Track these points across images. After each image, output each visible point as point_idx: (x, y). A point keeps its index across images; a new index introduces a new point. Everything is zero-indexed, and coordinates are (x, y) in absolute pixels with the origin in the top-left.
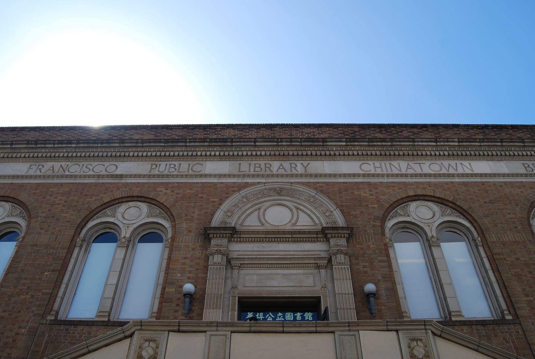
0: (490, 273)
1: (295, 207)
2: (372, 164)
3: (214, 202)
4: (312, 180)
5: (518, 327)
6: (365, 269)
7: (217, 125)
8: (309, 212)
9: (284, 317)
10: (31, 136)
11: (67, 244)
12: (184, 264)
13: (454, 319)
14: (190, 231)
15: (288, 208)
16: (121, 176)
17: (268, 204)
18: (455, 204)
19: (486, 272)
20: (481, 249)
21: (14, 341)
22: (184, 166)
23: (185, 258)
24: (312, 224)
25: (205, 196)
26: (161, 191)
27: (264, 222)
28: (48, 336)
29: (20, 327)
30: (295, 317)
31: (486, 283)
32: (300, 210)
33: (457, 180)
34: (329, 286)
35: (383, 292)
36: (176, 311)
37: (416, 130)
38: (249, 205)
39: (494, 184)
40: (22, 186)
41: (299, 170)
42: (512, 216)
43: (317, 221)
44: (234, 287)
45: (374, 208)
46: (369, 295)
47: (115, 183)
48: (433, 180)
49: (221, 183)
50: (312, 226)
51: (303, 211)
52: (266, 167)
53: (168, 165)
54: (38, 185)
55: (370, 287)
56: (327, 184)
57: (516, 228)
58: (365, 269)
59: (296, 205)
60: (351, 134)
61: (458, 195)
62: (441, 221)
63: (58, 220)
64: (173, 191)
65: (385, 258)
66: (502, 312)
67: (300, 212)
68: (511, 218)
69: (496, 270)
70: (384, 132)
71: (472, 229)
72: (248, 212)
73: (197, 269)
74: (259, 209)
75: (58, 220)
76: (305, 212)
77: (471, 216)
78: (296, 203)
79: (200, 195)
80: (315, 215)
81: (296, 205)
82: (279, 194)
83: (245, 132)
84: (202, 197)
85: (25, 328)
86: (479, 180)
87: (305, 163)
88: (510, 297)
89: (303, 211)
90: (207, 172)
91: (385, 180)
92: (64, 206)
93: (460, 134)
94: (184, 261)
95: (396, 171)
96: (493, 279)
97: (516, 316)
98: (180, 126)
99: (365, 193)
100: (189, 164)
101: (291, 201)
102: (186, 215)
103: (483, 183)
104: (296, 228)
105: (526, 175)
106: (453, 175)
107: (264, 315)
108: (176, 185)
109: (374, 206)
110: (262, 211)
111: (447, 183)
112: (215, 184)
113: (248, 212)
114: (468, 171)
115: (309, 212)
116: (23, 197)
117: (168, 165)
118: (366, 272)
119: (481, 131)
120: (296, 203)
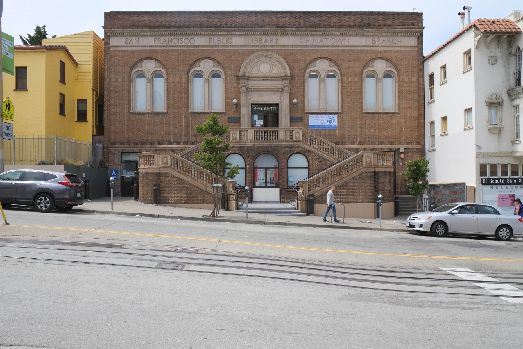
2: (305, 39)
3: (239, 60)
6: (295, 92)
7: (236, 12)
9: (266, 109)
10: (147, 19)
11: (186, 82)
12: (231, 90)
15: (268, 63)
16: (198, 46)
17: (261, 62)
18: (335, 62)
21: (181, 120)
22: (224, 39)
23: (231, 87)
25: (235, 57)
26: (217, 54)
29: (181, 115)
30: (270, 109)
33: (340, 49)
35: (300, 101)
36: (231, 108)
37: (329, 15)
38: (254, 63)
39: (355, 51)
40: (155, 51)
41: (274, 42)
42: (357, 68)
43: (280, 72)
45: (302, 64)
47: (196, 50)
48: (330, 49)
49: (241, 50)
54: (163, 50)
55: (295, 101)
57: (356, 74)
58: (295, 92)
64: (221, 55)
67: (273, 66)
68: (356, 70)
73: (236, 92)
76: (275, 66)
78: (272, 62)
79: (233, 57)
81: (272, 62)
83: (250, 16)
84: (234, 58)
87: (277, 38)
90: (234, 44)
91: (310, 48)
92: (178, 63)
94: (231, 88)
95: (315, 44)
98: (218, 12)
99: (300, 56)
102: (229, 67)
103: (351, 51)
104: (271, 74)
105: (371, 46)
106: (339, 46)
107: (260, 108)
108: (222, 51)
110: (259, 65)
111: (335, 50)
114: (346, 44)
116: (158, 58)
118: (295, 93)
120: (272, 62)
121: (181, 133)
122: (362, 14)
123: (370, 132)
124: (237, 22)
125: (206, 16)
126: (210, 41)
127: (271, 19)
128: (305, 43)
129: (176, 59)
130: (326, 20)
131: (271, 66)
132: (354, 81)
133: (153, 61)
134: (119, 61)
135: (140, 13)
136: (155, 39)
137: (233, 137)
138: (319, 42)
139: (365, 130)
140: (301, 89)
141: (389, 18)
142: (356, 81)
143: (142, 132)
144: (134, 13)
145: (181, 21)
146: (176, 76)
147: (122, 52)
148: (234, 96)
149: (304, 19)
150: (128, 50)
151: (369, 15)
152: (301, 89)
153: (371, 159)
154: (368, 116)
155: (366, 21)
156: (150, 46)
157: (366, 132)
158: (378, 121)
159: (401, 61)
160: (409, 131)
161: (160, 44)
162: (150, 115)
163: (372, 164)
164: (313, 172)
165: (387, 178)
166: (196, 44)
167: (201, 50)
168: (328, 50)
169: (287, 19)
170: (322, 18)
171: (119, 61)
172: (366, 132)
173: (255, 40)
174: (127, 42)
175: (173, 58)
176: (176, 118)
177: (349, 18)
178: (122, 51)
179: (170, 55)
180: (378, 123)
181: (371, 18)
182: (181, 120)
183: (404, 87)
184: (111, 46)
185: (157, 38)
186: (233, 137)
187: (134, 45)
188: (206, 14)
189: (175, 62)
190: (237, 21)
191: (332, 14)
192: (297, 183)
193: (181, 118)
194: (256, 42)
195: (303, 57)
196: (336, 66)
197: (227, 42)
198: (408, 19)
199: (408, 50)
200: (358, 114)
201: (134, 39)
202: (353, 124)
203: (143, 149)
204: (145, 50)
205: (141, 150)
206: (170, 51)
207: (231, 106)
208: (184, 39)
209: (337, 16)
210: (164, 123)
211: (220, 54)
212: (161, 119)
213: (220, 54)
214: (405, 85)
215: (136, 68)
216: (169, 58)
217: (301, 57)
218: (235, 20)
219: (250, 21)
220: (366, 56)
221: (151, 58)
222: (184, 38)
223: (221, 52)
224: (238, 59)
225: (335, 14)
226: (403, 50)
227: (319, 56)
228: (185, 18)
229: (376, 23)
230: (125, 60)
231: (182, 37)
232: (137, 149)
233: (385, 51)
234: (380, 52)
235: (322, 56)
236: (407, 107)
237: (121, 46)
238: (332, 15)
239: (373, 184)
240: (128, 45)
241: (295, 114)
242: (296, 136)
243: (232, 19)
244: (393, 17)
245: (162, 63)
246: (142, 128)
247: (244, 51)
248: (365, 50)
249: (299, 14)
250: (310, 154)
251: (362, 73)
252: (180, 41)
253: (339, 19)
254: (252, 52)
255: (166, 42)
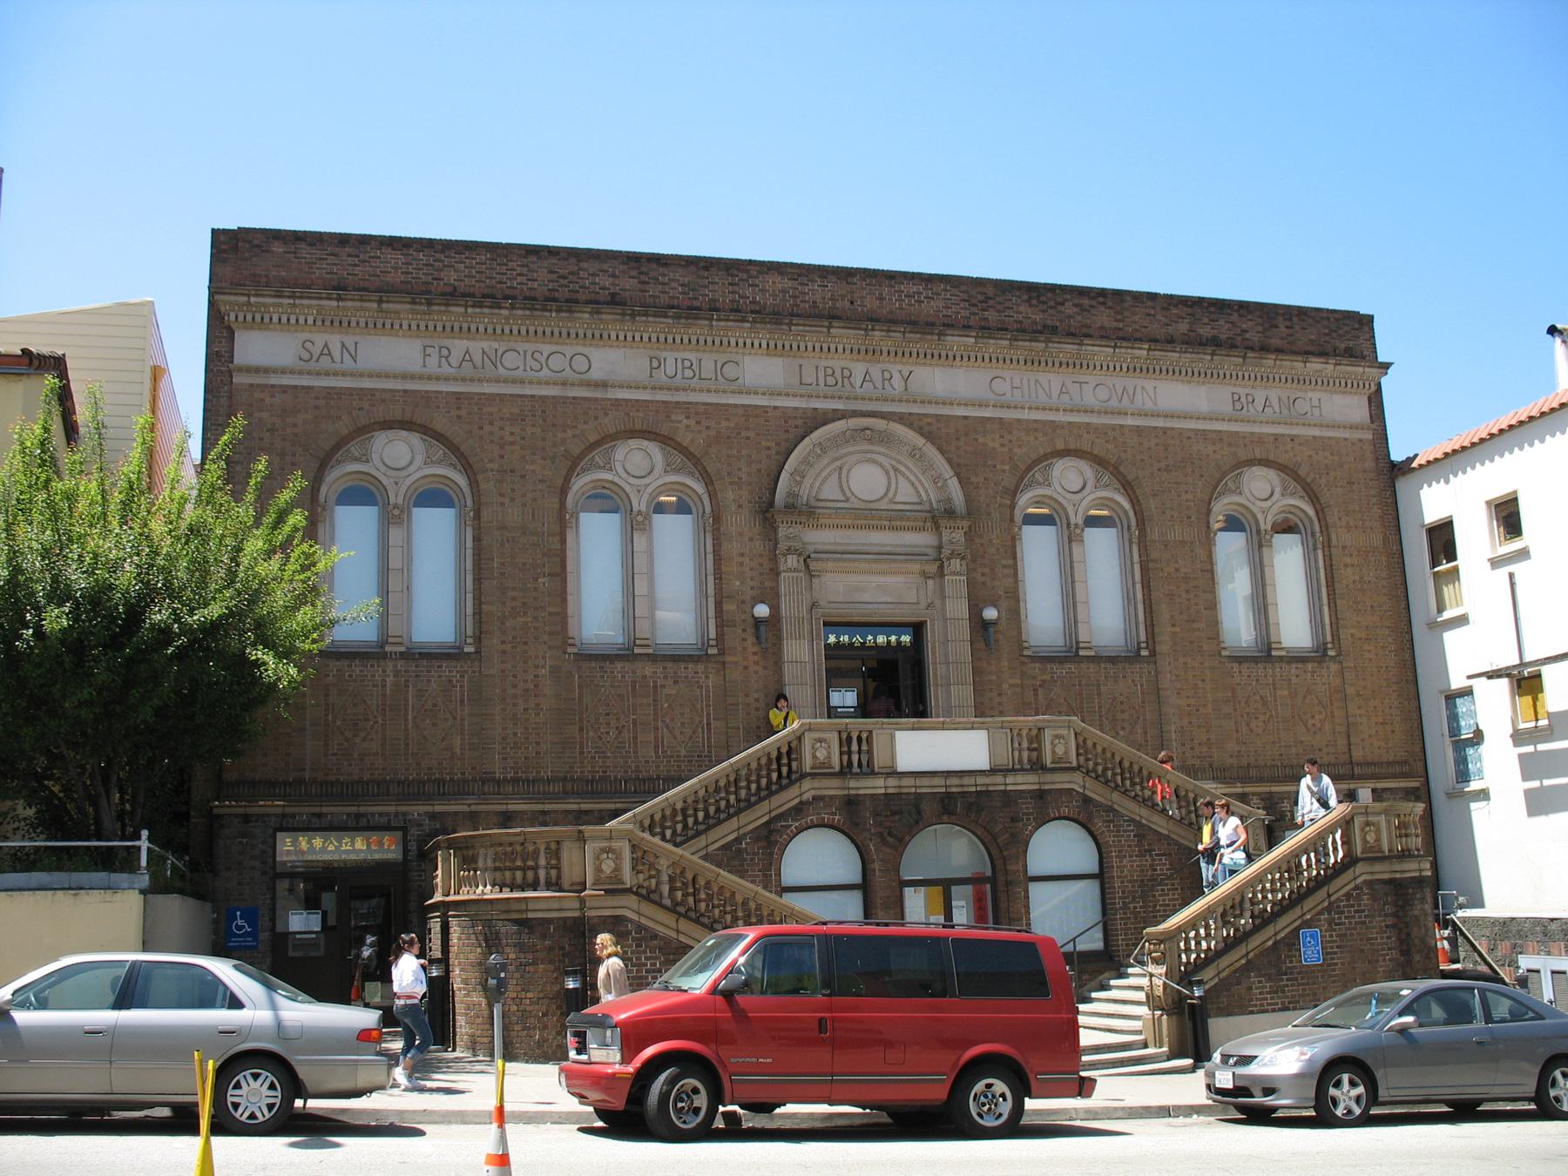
0: (1139, 586)
1: (896, 470)
2: (1008, 380)
3: (768, 448)
4: (915, 409)
5: (1152, 666)
6: (984, 579)
7: (750, 262)
8: (913, 479)
10: (392, 268)
12: (741, 564)
13: (1081, 653)
14: (740, 506)
16: (603, 385)
17: (853, 458)
19: (1134, 584)
20: (1135, 548)
21: (536, 686)
23: (742, 555)
24: (917, 500)
25: (752, 434)
26: (680, 422)
27: (849, 495)
28: (580, 677)
29: (536, 667)
31: (1128, 598)
32: (900, 472)
33: (1130, 421)
34: (938, 603)
36: (744, 640)
37: (1086, 302)
38: (826, 461)
39: (1181, 432)
40: (427, 397)
41: (896, 386)
42: (1190, 496)
44: (814, 605)
45: (1004, 471)
46: (986, 625)
47: (596, 399)
48: (1093, 419)
50: (913, 504)
51: (904, 475)
52: (843, 377)
53: (679, 362)
54: (458, 396)
55: (990, 613)
56: (938, 418)
57: (1189, 517)
58: (984, 579)
59: (893, 462)
60: (981, 302)
61: (1125, 451)
62: (1093, 496)
63: (523, 477)
64: (698, 423)
65: (1011, 562)
66: (1139, 644)
67: (900, 478)
68: (1187, 501)
69: (1146, 585)
70: (1034, 302)
71: (1132, 514)
72: (824, 474)
73: (761, 574)
74: (841, 469)
75: (523, 477)
76: (907, 478)
77: (1134, 492)
79: (744, 434)
80: (922, 484)
81: (893, 462)
82: (869, 441)
83: (801, 284)
84: (748, 438)
85: (544, 667)
86: (1160, 423)
88: (1153, 626)
89: (904, 475)
91: (1026, 415)
92: (523, 448)
93: (1154, 316)
94: (740, 559)
95: (1043, 398)
96: (1139, 596)
97: (1153, 653)
98: (680, 258)
100: (716, 362)
101: (887, 456)
102: (729, 474)
103: (1165, 431)
108: (702, 408)
109: (1004, 467)
111: (1113, 427)
112: (764, 409)
113: (824, 474)
114: (1149, 405)
115: (913, 479)
116: (440, 423)
117: (679, 362)
118: (984, 583)
119: (1189, 310)
121: (538, 743)
122: (1191, 306)
123: (1252, 731)
124: (754, 302)
125: (634, 273)
126: (652, 368)
127: (881, 298)
128: (1009, 395)
129: (512, 434)
130: (1073, 317)
131: (893, 477)
132: (1183, 542)
133: (415, 438)
134: (272, 430)
135: (364, 240)
136: (425, 347)
137: (814, 757)
138: (1055, 394)
139: (1236, 723)
140: (1004, 567)
141: (1276, 327)
142: (1192, 543)
143: (364, 740)
144: (343, 239)
145: (535, 285)
146: (512, 500)
147: (285, 392)
148: (752, 588)
149: (999, 307)
150: (311, 388)
151: (1212, 309)
152: (1004, 567)
153: (1378, 832)
154: (1240, 672)
155: (1205, 331)
156: (405, 376)
157: (1237, 731)
158: (1274, 689)
159: (1328, 474)
160: (1376, 723)
161: (446, 370)
162: (400, 664)
163: (1383, 852)
164: (1123, 892)
165: (881, 898)
166: (595, 374)
167: (618, 403)
168: (1088, 424)
169: (937, 304)
170: (1059, 307)
171: (272, 430)
172: (1237, 731)
173: (826, 376)
174: (306, 356)
175: (502, 429)
176: (515, 676)
177: (1149, 315)
178: (285, 389)
179: (491, 414)
180: (1275, 696)
181: (1222, 322)
182: (536, 686)
183: (1346, 566)
184: (241, 370)
185: (437, 342)
186: (814, 757)
187: (338, 366)
188: (633, 264)
189: (513, 443)
190: (754, 298)
191: (1094, 298)
192: (1074, 940)
193: (536, 676)
194: (831, 381)
195: (1002, 445)
196: (1118, 485)
197: (719, 377)
198: (1334, 334)
199: (1346, 439)
200: (1206, 665)
201: (339, 345)
202: (1192, 701)
203: (373, 814)
204: (384, 390)
205: (365, 815)
206: (491, 397)
207: (744, 630)
208: (545, 355)
209: (1110, 304)
210: (462, 701)
211: (692, 422)
212: (450, 681)
213: (692, 422)
214: (1348, 560)
215: (339, 462)
216: (487, 428)
217: (997, 445)
218: (749, 292)
219: (802, 301)
220: (1215, 452)
221: (406, 425)
222: (547, 349)
223: (697, 413)
224: (764, 444)
225: (1101, 299)
226: (1329, 438)
227: (1060, 446)
228: (554, 272)
229: (1239, 338)
230: (295, 425)
231: (540, 347)
232: (349, 815)
233: (1276, 439)
234: (1259, 440)
235: (1072, 447)
236: (1360, 639)
237: (283, 371)
238: (1094, 303)
239: (1393, 926)
240: (312, 366)
241: (989, 664)
242: (1054, 752)
243: (736, 288)
244: (1288, 323)
245: (453, 448)
246: (367, 720)
247: (786, 415)
248: (1210, 431)
249: (980, 289)
250: (1110, 821)
251: (1209, 512)
252: (530, 362)
253: (1119, 317)
254: (819, 419)
255: (471, 360)
